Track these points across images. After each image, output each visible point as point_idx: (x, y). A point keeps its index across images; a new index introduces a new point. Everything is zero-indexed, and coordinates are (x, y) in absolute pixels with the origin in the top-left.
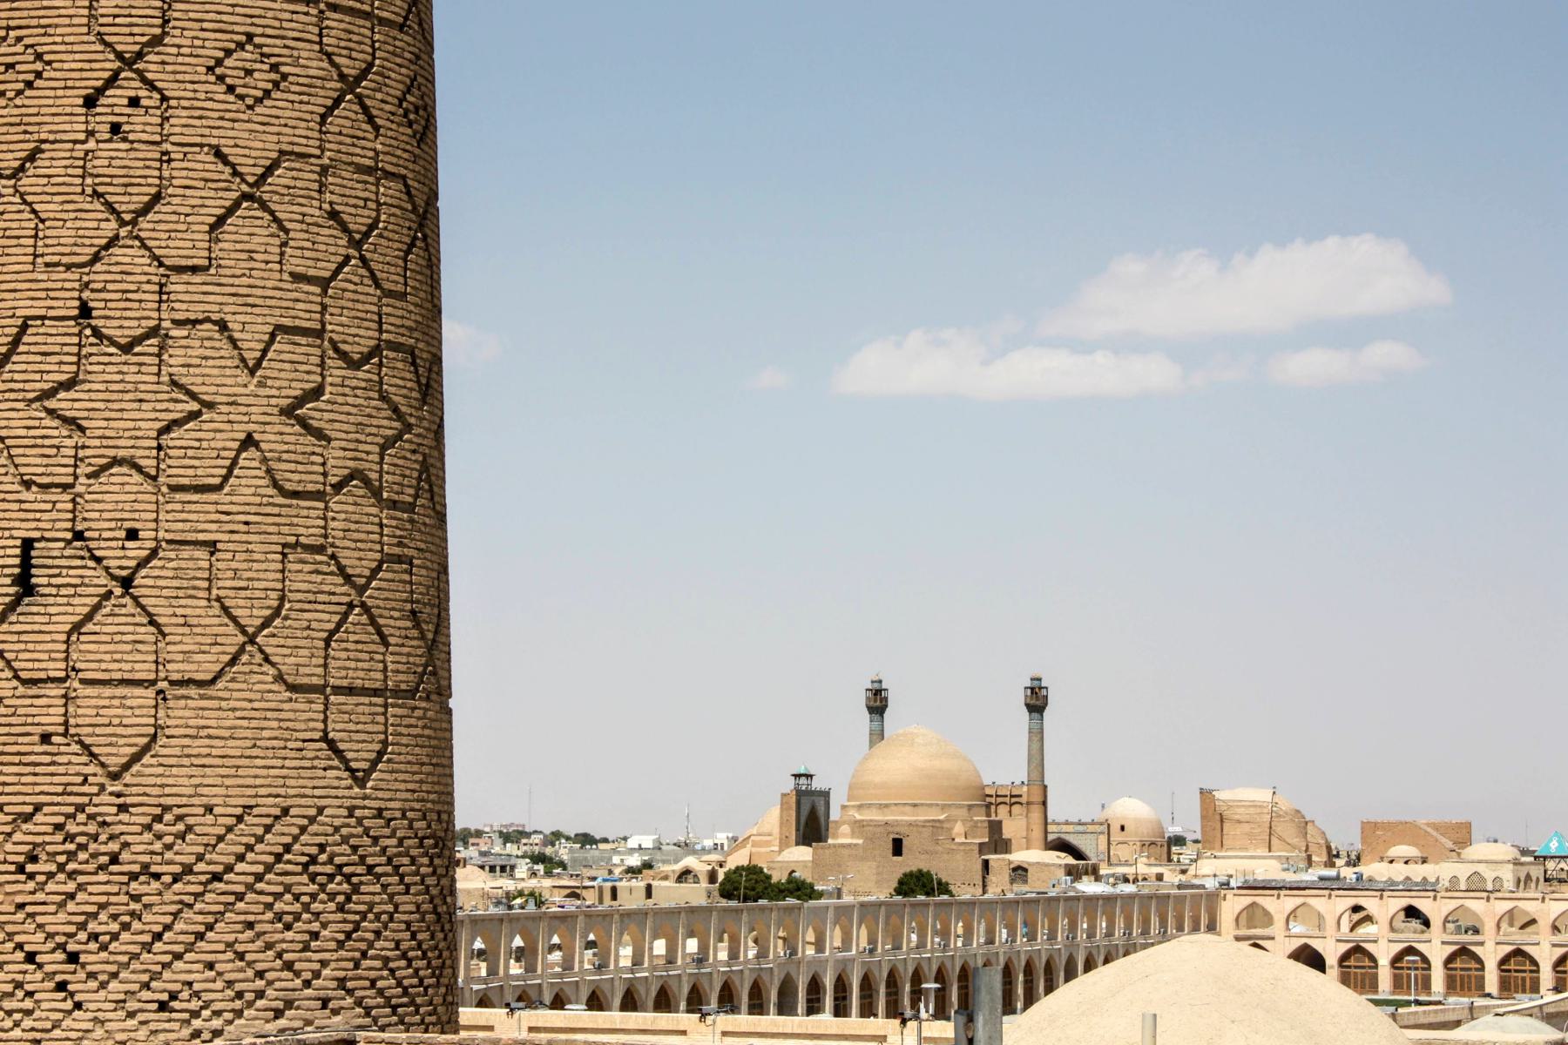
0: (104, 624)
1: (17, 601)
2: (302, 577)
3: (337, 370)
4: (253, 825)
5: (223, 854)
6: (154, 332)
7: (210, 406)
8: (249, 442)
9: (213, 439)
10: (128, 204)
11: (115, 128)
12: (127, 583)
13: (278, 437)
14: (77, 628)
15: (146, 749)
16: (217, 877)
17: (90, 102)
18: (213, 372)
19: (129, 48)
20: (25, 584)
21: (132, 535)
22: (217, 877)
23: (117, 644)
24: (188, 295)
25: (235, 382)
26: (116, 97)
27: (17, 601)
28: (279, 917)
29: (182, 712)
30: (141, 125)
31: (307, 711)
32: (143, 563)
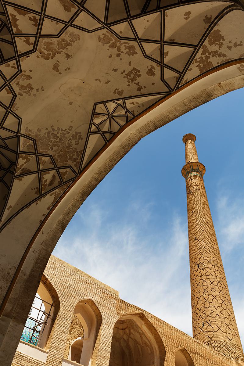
0: (209, 327)
1: (203, 327)
2: (223, 324)
3: (223, 310)
4: (222, 342)
5: (220, 344)
6: (209, 307)
7: (214, 312)
8: (217, 314)
9: (215, 314)
10: (206, 299)
11: (205, 294)
12: (210, 324)
13: (219, 314)
14: (207, 328)
15: (213, 336)
16: (220, 346)
17: (203, 293)
18: (214, 309)
19: (205, 289)
20: (203, 325)
21: (210, 321)
22: (220, 346)
23: (210, 329)
24: (211, 304)
25: (215, 310)
26: (205, 292)
27: (203, 327)
28: (225, 350)
29: (215, 333)
30: (206, 294)
31: (225, 334)
32: (211, 323)
